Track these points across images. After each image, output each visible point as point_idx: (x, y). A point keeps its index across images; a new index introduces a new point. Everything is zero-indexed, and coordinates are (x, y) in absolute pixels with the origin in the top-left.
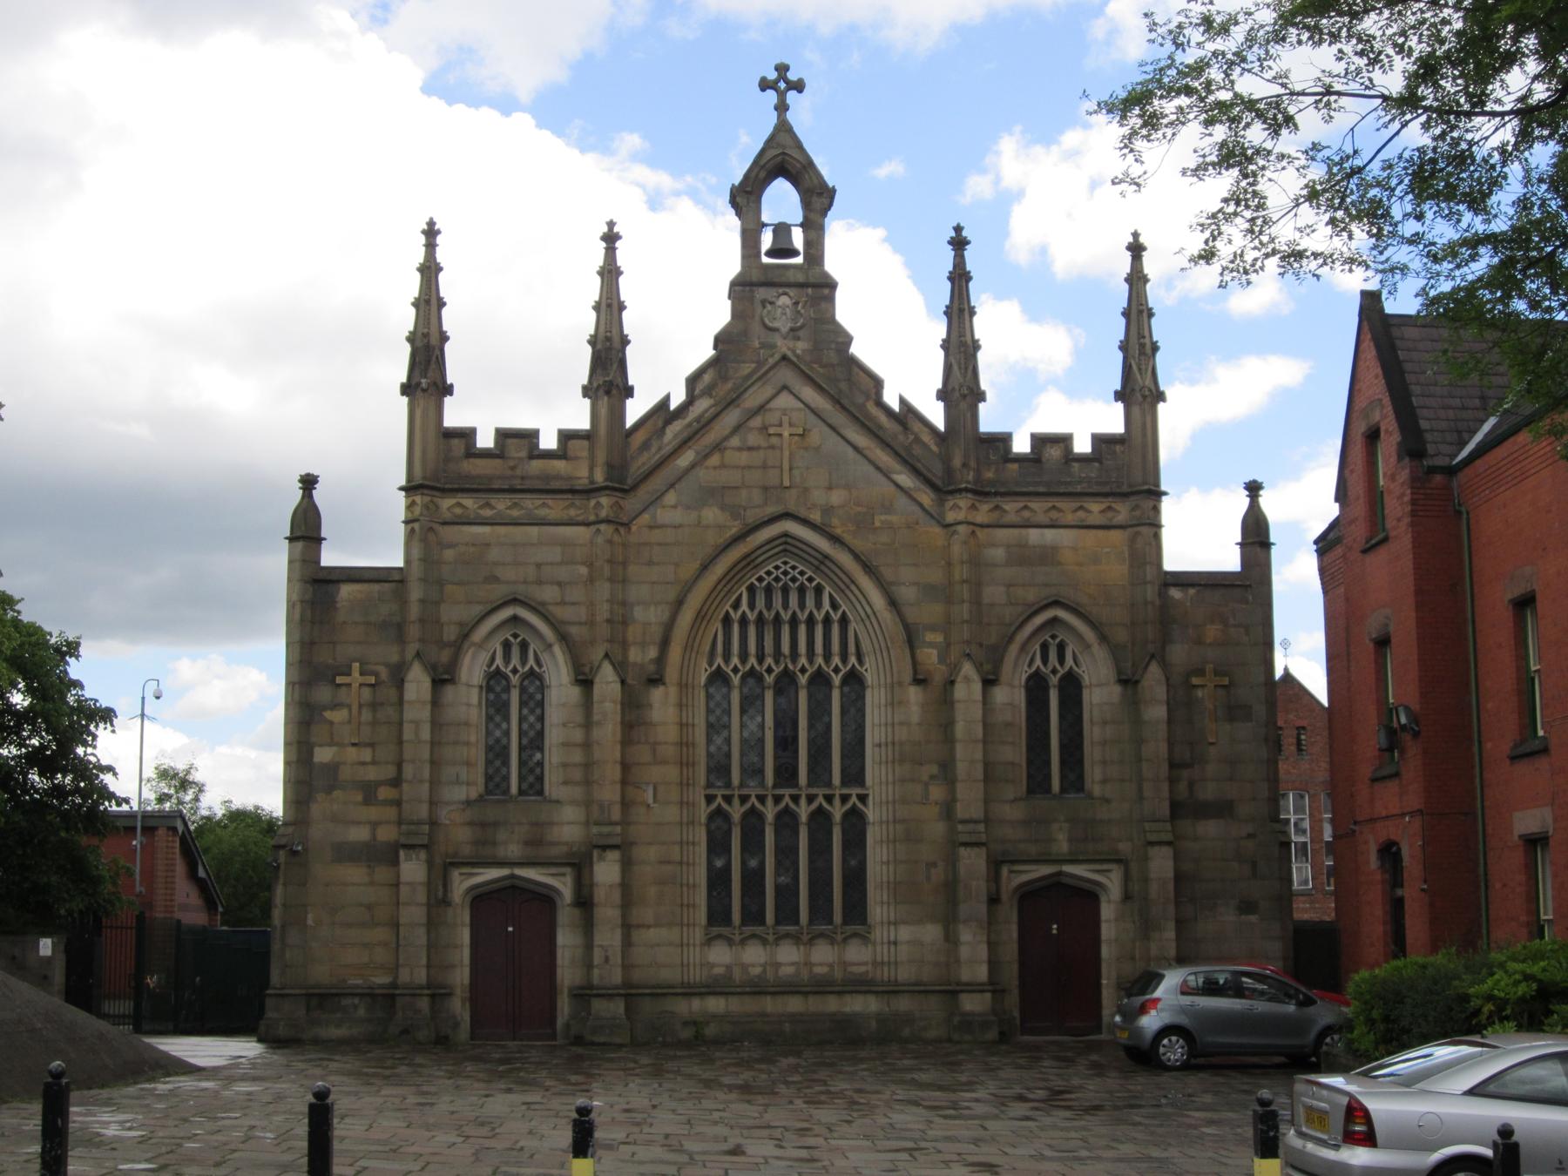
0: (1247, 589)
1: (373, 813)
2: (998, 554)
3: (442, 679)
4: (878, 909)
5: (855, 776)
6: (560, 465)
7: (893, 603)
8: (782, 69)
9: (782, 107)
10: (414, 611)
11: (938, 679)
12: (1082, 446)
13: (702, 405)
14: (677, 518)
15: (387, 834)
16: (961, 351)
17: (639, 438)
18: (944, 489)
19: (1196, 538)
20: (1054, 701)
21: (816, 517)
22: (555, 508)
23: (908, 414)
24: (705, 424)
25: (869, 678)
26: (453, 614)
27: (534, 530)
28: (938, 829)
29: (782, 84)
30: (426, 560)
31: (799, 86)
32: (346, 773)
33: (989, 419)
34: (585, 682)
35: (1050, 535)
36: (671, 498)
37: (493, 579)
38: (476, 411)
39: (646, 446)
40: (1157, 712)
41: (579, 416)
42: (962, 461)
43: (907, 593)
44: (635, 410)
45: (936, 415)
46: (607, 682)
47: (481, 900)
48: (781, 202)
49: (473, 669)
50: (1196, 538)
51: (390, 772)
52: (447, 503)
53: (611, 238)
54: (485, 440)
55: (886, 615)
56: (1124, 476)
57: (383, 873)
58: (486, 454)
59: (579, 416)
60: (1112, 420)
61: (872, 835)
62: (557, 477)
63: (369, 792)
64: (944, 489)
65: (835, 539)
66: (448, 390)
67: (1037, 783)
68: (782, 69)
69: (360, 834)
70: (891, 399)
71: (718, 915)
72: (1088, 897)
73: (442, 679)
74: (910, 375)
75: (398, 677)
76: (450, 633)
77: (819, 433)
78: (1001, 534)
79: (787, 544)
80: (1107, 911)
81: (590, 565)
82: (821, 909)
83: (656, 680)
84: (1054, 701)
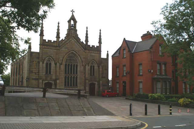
0: (107, 59)
1: (36, 75)
2: (89, 55)
3: (43, 63)
4: (78, 85)
5: (77, 73)
6: (53, 44)
7: (81, 59)
8: (73, 10)
9: (73, 13)
10: (40, 56)
11: (84, 66)
12: (96, 47)
13: (66, 40)
14: (64, 50)
15: (37, 77)
16: (87, 37)
17: (60, 42)
18: (85, 49)
19: (104, 56)
20: (92, 68)
21: (75, 51)
22: (53, 48)
23: (82, 42)
24: (66, 42)
25: (78, 65)
26: (44, 57)
27: (51, 50)
28: (84, 78)
29: (73, 11)
30: (42, 52)
31: (74, 12)
32: (34, 71)
33: (89, 44)
34: (56, 64)
35: (93, 54)
36: (63, 48)
37: (47, 54)
38: (46, 38)
39: (61, 43)
40: (101, 69)
41: (55, 40)
42: (86, 47)
43: (82, 58)
44: (60, 39)
45: (85, 43)
46: (58, 64)
47: (45, 84)
48: (72, 22)
49: (45, 62)
50: (104, 56)
51: (38, 71)
52: (43, 46)
53: (59, 23)
54: (47, 41)
55: (80, 60)
56: (98, 49)
57: (37, 81)
58: (47, 42)
59: (55, 40)
60: (98, 45)
61: (78, 79)
62: (53, 45)
63: (36, 73)
64: (85, 49)
65: (76, 53)
66: (44, 36)
67: (91, 75)
68: (73, 10)
69: (35, 77)
70: (81, 41)
71: (65, 85)
72: (94, 84)
73: (43, 63)
74: (83, 39)
75: (39, 63)
76: (43, 59)
77: (75, 44)
78: (89, 54)
79: (72, 53)
80: (96, 86)
81: (56, 53)
82: (74, 85)
83: (61, 64)
84: (92, 68)
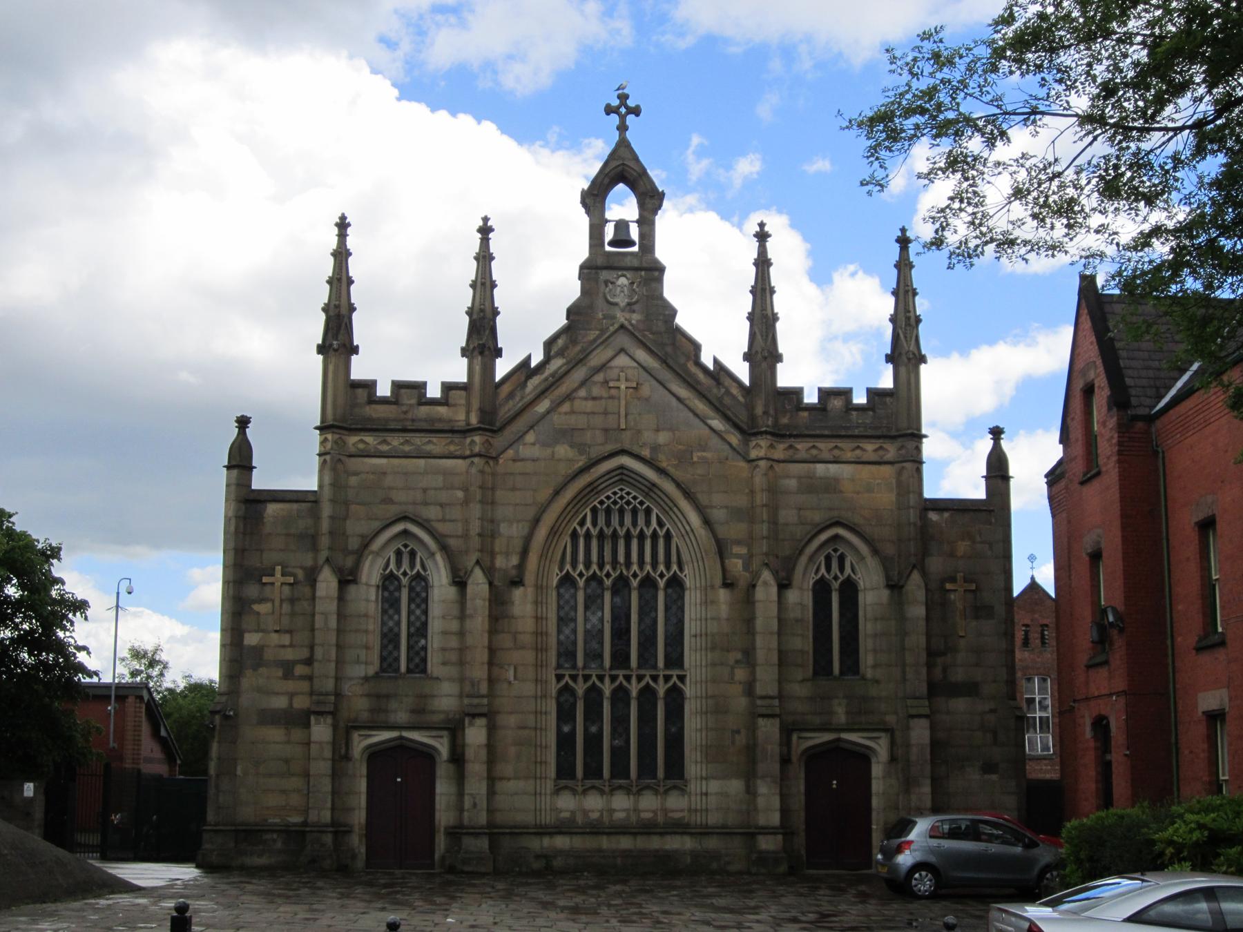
0: (993, 511)
1: (290, 685)
2: (792, 483)
3: (347, 579)
4: (693, 766)
5: (675, 660)
6: (442, 410)
7: (707, 522)
9: (622, 128)
10: (325, 525)
11: (742, 583)
13: (556, 364)
14: (535, 455)
15: (301, 703)
16: (763, 322)
17: (506, 389)
18: (748, 432)
19: (952, 473)
20: (835, 601)
21: (646, 453)
22: (437, 444)
23: (721, 371)
24: (558, 378)
25: (688, 583)
26: (356, 528)
27: (422, 462)
31: (636, 111)
32: (269, 655)
33: (785, 378)
34: (460, 583)
35: (833, 468)
36: (530, 437)
38: (378, 364)
39: (511, 395)
40: (917, 611)
41: (458, 371)
42: (761, 409)
43: (718, 515)
44: (503, 368)
45: (742, 371)
46: (478, 584)
47: (376, 755)
49: (371, 572)
50: (952, 473)
51: (305, 653)
52: (352, 440)
54: (384, 390)
56: (891, 421)
57: (298, 734)
58: (384, 401)
59: (458, 371)
61: (688, 707)
62: (440, 420)
63: (287, 669)
64: (748, 432)
65: (661, 471)
66: (355, 350)
67: (822, 668)
68: (623, 98)
69: (280, 703)
70: (707, 360)
71: (565, 771)
72: (862, 758)
73: (347, 579)
74: (722, 340)
75: (312, 577)
76: (354, 543)
78: (795, 468)
80: (877, 770)
82: (647, 768)
83: (517, 582)
84: (835, 601)
